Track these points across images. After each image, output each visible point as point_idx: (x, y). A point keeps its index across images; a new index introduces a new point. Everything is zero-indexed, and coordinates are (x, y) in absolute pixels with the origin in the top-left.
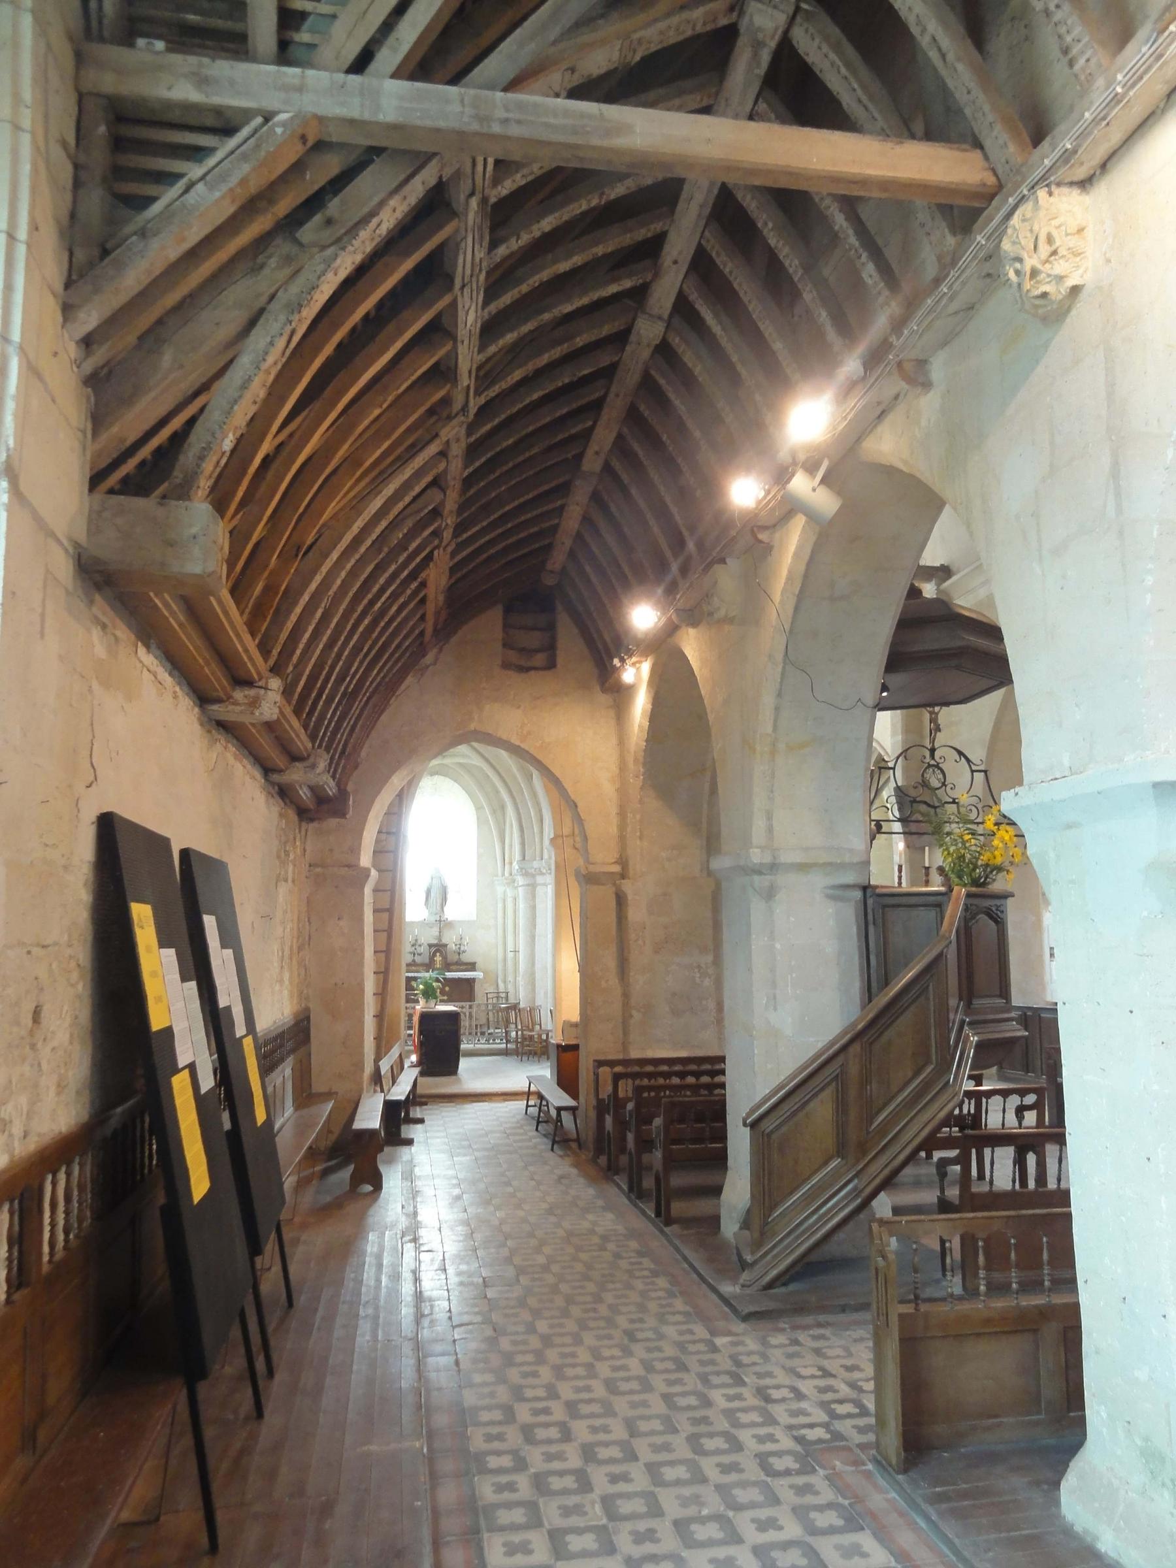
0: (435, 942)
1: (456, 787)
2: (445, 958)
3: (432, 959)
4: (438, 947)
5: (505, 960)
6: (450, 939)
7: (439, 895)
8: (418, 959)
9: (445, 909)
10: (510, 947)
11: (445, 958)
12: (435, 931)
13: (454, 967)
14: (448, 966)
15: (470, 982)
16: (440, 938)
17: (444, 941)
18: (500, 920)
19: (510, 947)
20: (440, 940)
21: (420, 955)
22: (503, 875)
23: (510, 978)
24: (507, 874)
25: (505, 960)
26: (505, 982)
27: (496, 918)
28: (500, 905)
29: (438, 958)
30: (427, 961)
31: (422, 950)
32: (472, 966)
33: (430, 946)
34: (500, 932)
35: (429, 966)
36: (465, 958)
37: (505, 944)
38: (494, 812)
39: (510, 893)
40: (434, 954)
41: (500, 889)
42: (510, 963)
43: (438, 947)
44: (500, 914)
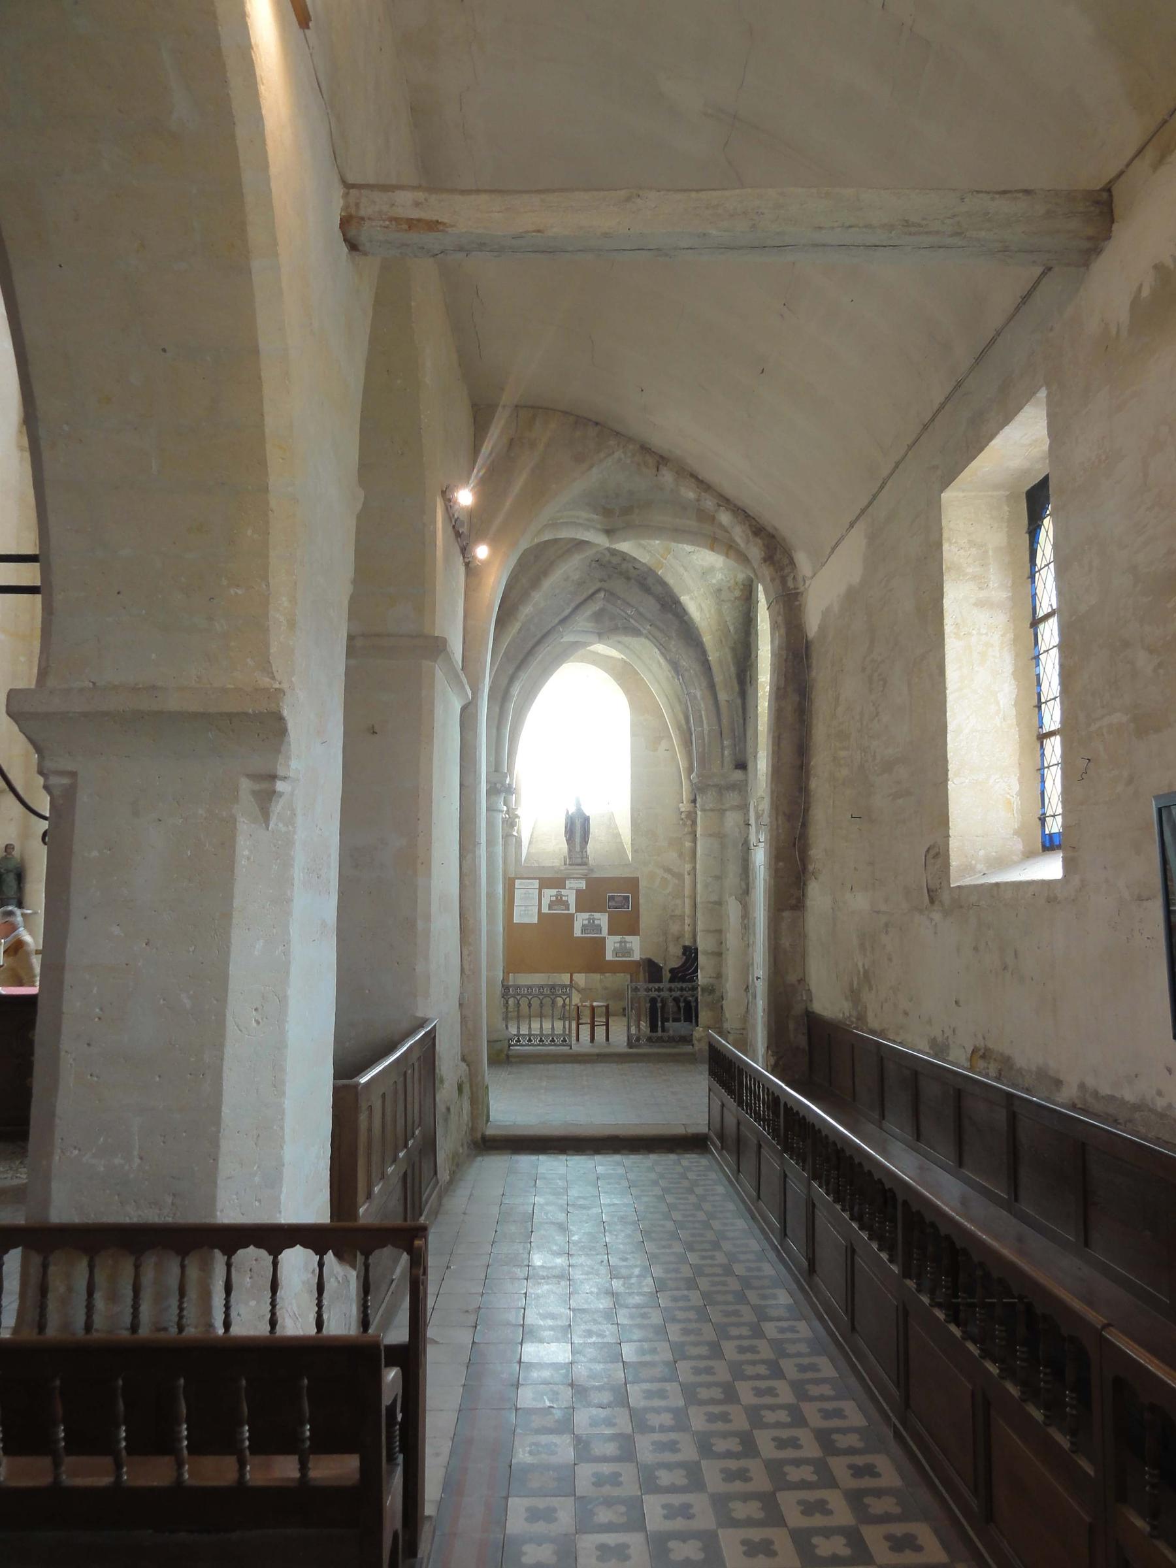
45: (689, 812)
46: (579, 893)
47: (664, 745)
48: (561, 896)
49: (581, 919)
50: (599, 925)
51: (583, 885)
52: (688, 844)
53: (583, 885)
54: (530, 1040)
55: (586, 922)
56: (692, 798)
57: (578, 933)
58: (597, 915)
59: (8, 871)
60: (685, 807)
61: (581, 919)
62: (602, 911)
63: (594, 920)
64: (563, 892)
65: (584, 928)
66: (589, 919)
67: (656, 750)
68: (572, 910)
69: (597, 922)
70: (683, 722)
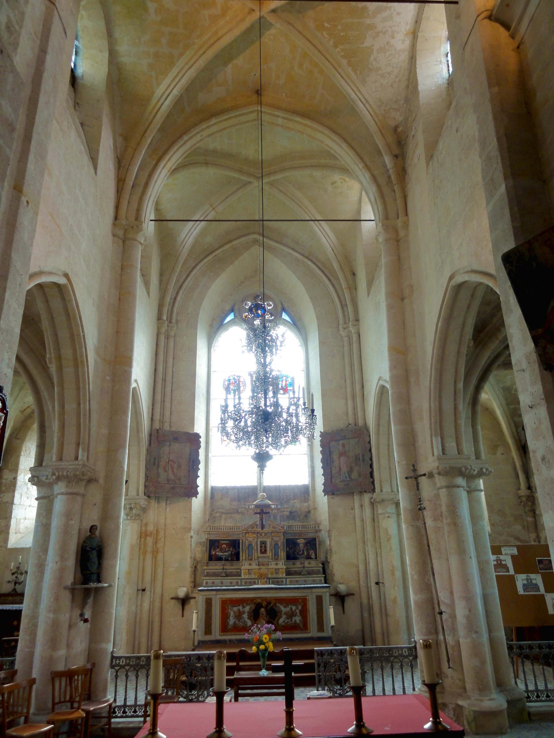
45: (529, 496)
46: (513, 557)
47: (500, 450)
48: (501, 561)
49: (521, 580)
50: (536, 585)
51: (515, 551)
52: (530, 519)
53: (515, 551)
54: (538, 696)
55: (525, 582)
56: (528, 486)
57: (521, 591)
58: (532, 576)
59: (93, 549)
60: (523, 491)
61: (521, 580)
62: (537, 572)
63: (531, 580)
64: (502, 557)
65: (526, 587)
66: (527, 579)
67: (495, 454)
68: (512, 572)
69: (534, 582)
70: (516, 434)
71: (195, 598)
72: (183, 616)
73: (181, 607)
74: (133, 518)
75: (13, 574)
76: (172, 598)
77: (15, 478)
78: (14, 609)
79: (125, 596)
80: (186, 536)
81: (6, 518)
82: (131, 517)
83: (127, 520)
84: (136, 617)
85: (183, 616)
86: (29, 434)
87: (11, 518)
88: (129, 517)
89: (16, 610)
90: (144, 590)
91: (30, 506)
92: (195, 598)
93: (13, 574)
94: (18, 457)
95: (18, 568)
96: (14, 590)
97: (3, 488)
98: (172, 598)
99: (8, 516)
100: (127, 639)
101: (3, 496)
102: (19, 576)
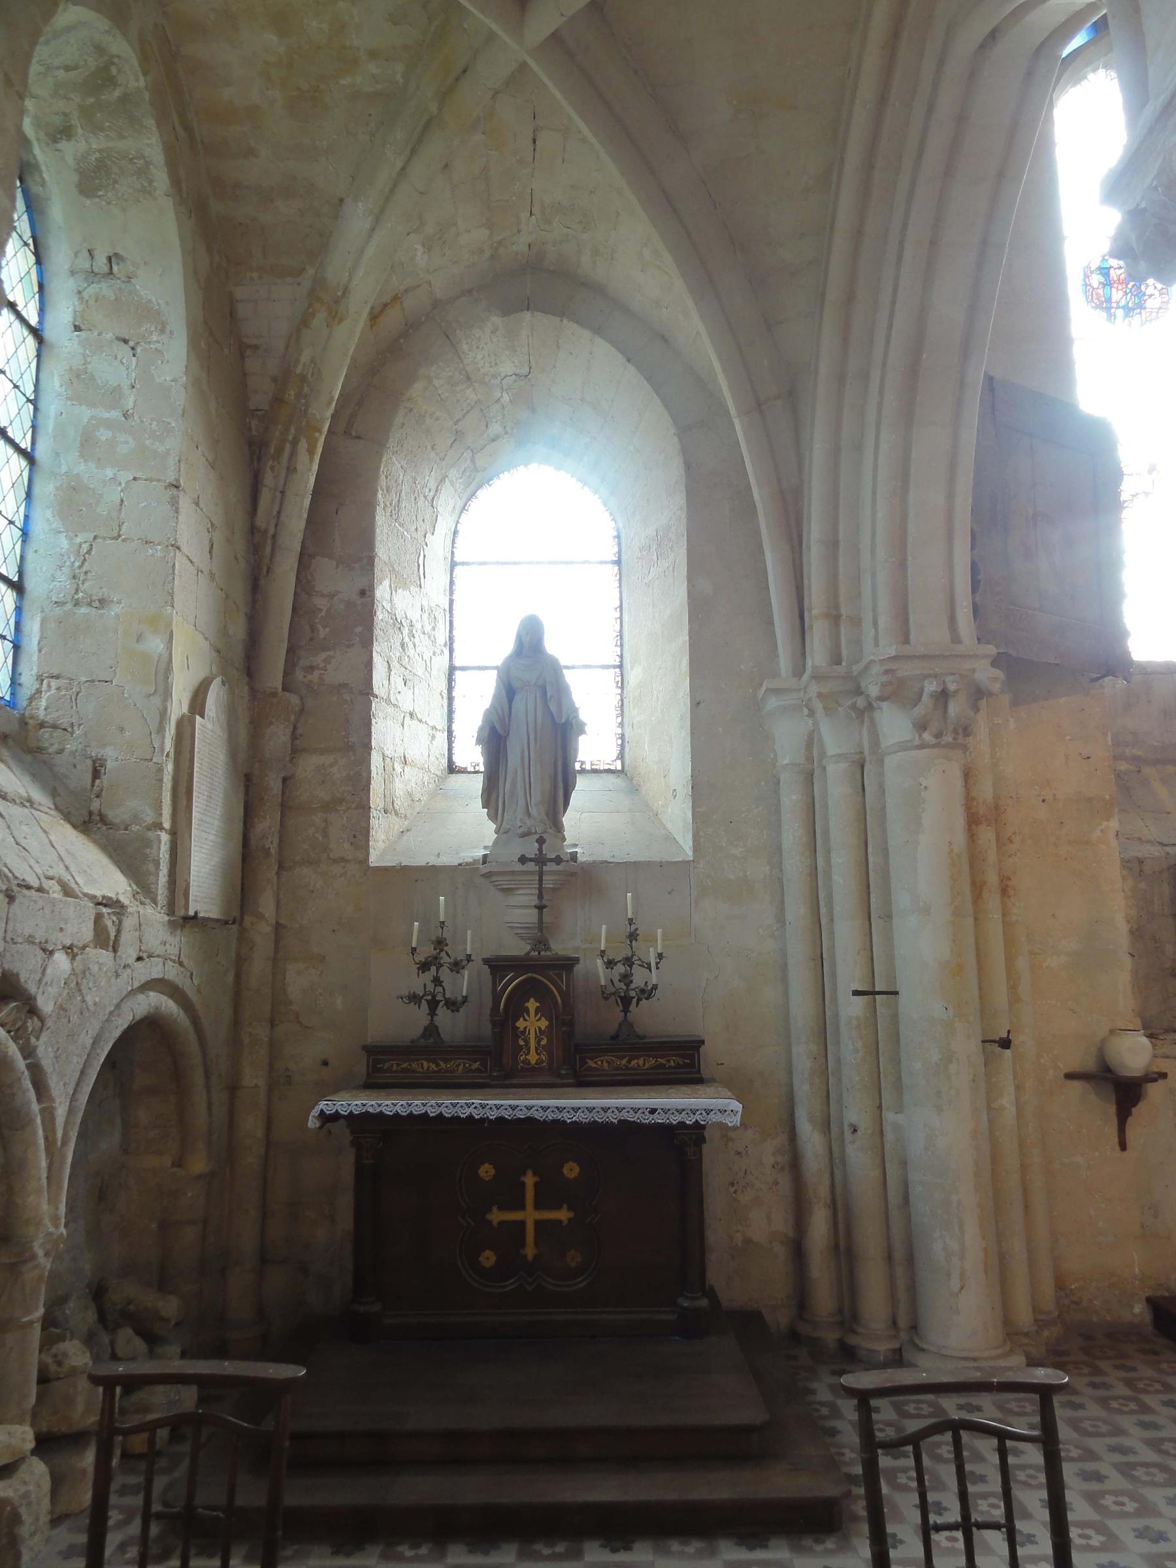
0: (517, 948)
1: (602, 347)
2: (562, 1020)
3: (505, 1018)
4: (534, 975)
5: (823, 1031)
6: (587, 937)
7: (530, 738)
8: (451, 1025)
9: (569, 819)
10: (848, 973)
11: (562, 1020)
12: (520, 910)
13: (600, 1064)
14: (575, 1064)
15: (682, 1144)
16: (541, 936)
17: (560, 947)
18: (794, 864)
19: (848, 973)
20: (541, 943)
21: (453, 1005)
22: (799, 669)
23: (856, 1111)
24: (817, 656)
25: (823, 1031)
26: (825, 1125)
27: (777, 850)
28: (791, 798)
29: (533, 1023)
30: (487, 1029)
31: (463, 984)
32: (682, 1062)
33: (498, 966)
34: (796, 910)
35: (494, 1063)
36: (651, 1019)
37: (820, 961)
38: (757, 407)
39: (835, 741)
40: (516, 1008)
41: (787, 738)
42: (850, 1049)
43: (534, 975)
44: (792, 835)
71: (1164, 1076)
72: (1123, 1146)
73: (1112, 1110)
74: (948, 738)
75: (424, 967)
76: (1070, 1076)
77: (367, 593)
78: (493, 1115)
79: (953, 1068)
80: (1098, 832)
81: (349, 748)
82: (938, 735)
83: (922, 746)
84: (995, 1158)
85: (1123, 1146)
86: (398, 420)
87: (368, 747)
88: (927, 736)
89: (501, 1119)
90: (1005, 1043)
91: (411, 715)
92: (1164, 1076)
93: (424, 967)
94: (369, 508)
95: (440, 943)
96: (431, 1030)
97: (323, 632)
98: (1070, 1076)
99: (353, 739)
100: (985, 1250)
101: (327, 661)
102: (445, 974)
